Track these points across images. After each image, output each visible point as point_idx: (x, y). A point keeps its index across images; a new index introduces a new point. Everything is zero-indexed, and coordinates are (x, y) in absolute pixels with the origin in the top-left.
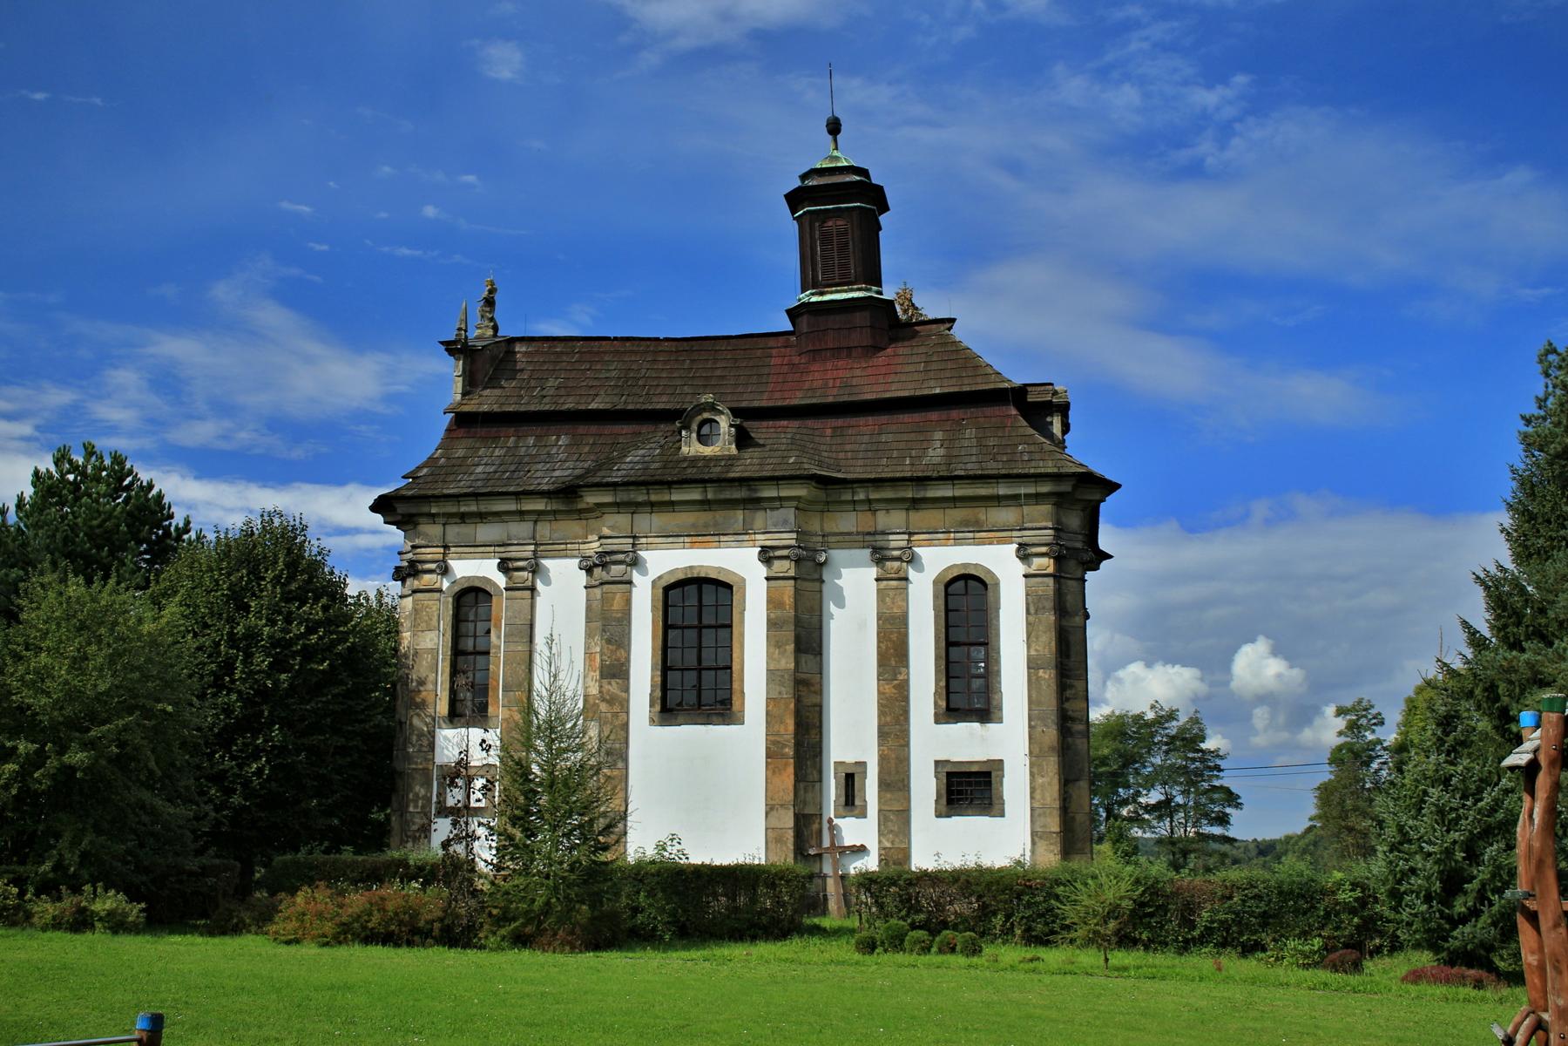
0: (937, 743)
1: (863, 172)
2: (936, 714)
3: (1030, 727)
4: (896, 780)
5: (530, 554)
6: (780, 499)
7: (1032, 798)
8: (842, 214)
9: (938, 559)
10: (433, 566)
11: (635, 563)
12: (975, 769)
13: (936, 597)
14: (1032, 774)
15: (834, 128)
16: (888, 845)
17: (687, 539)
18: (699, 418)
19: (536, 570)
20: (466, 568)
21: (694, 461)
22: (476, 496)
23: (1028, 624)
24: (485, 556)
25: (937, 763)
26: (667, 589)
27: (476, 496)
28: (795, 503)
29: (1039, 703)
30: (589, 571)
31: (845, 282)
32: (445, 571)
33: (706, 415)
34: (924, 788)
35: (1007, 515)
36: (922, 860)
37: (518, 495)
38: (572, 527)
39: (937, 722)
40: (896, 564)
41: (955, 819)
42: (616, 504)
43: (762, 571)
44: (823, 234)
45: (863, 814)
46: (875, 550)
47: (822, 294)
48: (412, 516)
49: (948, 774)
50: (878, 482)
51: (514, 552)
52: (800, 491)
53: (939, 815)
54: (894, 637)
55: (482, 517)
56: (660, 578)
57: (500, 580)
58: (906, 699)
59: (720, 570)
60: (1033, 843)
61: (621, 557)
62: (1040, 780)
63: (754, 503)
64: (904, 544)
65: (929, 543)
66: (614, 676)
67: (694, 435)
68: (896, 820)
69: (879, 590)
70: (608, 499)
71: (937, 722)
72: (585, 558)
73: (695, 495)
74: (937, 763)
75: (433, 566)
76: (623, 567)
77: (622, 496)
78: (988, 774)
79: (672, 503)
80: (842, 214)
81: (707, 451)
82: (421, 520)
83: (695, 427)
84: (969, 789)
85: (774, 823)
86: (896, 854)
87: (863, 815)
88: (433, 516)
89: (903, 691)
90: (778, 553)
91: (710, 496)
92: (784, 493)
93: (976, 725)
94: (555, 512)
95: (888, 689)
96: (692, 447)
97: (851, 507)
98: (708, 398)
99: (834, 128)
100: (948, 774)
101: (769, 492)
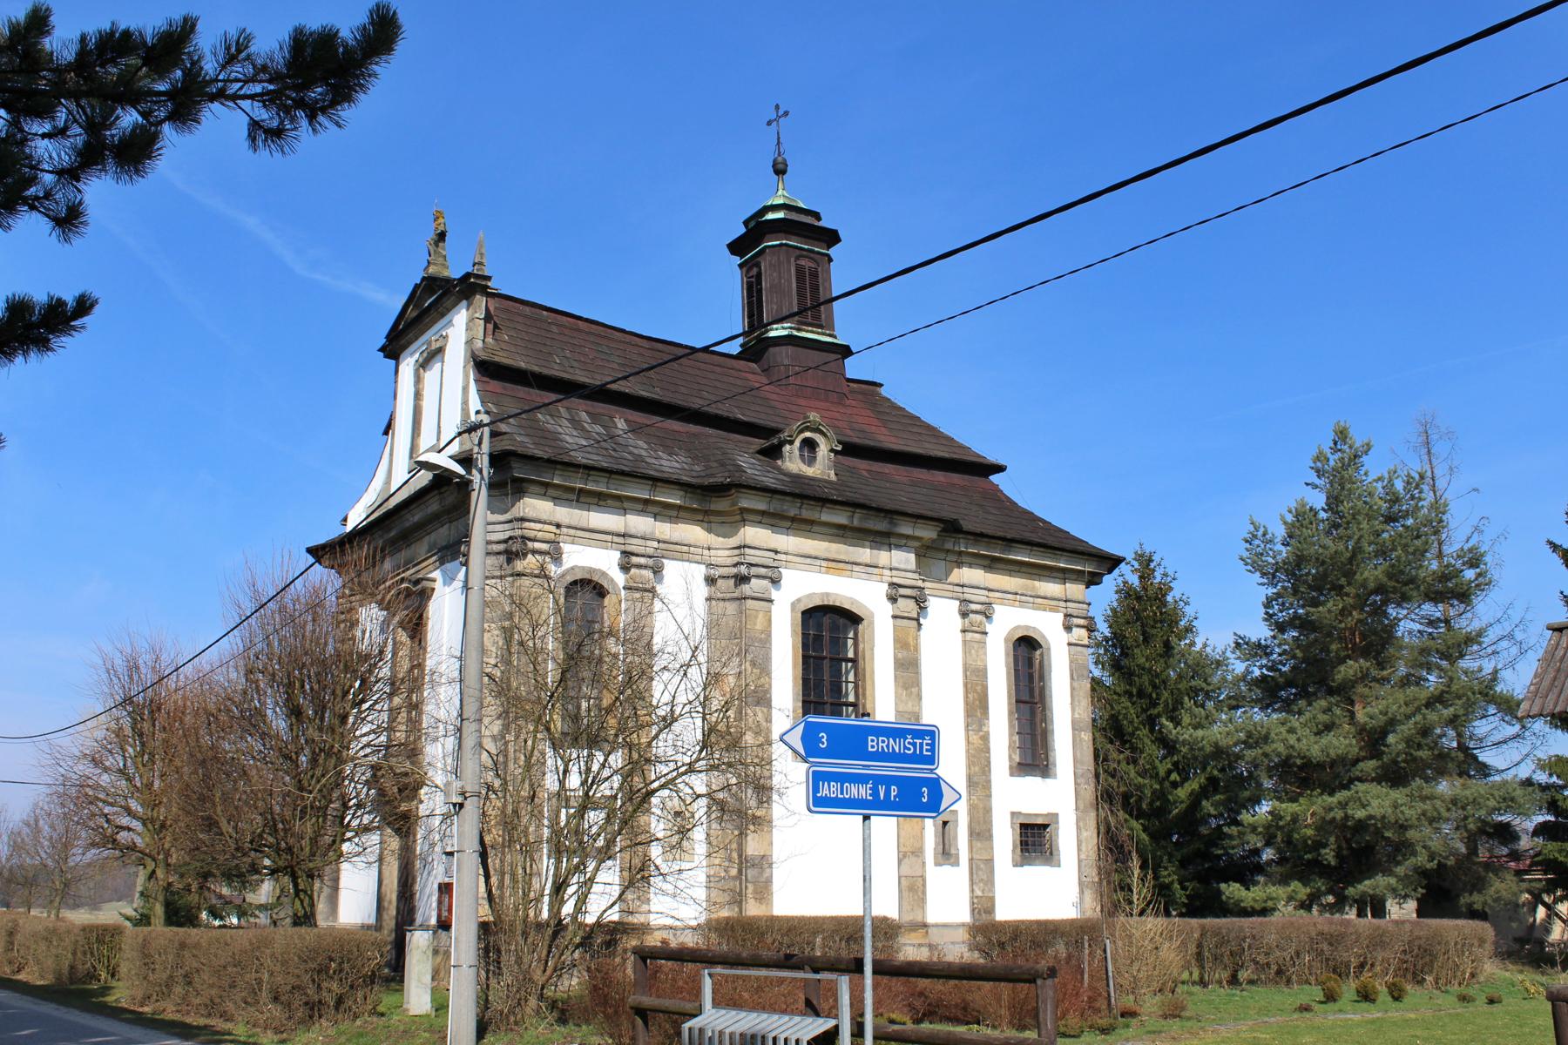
0: (1017, 796)
1: (817, 216)
2: (1011, 767)
3: (1076, 783)
4: (981, 832)
5: (650, 551)
6: (908, 537)
7: (1079, 850)
8: (784, 251)
9: (1008, 620)
10: (544, 547)
11: (775, 582)
12: (1040, 821)
13: (1007, 654)
14: (1078, 828)
15: (780, 170)
16: (979, 893)
17: (824, 564)
18: (808, 434)
19: (657, 571)
20: (580, 557)
21: (798, 478)
22: (609, 472)
23: (1073, 689)
24: (604, 545)
25: (1013, 814)
26: (804, 613)
27: (609, 472)
28: (917, 544)
29: (1082, 763)
30: (711, 581)
31: (818, 324)
32: (557, 557)
33: (808, 434)
34: (1004, 839)
35: (1051, 588)
36: (1005, 912)
37: (656, 481)
38: (692, 533)
39: (1012, 775)
40: (979, 618)
41: (1026, 868)
42: (763, 513)
43: (888, 606)
44: (798, 271)
45: (956, 863)
46: (964, 601)
47: (799, 330)
48: (523, 480)
49: (1022, 825)
50: (979, 537)
51: (634, 545)
52: (928, 533)
53: (1015, 865)
54: (979, 688)
55: (599, 500)
56: (799, 600)
57: (620, 578)
58: (988, 751)
59: (853, 601)
60: (1082, 892)
61: (763, 571)
62: (1085, 834)
63: (883, 539)
64: (983, 599)
65: (1002, 601)
66: (758, 703)
67: (797, 452)
68: (982, 872)
69: (965, 642)
70: (761, 506)
71: (1012, 775)
72: (709, 565)
73: (840, 518)
74: (1013, 814)
75: (544, 547)
76: (765, 582)
77: (775, 505)
78: (1045, 826)
79: (812, 522)
80: (784, 251)
81: (810, 471)
82: (533, 488)
83: (797, 443)
84: (1034, 839)
85: (906, 870)
86: (983, 905)
87: (956, 863)
88: (547, 485)
89: (985, 738)
90: (902, 591)
91: (856, 523)
92: (918, 533)
93: (1039, 779)
94: (679, 508)
95: (974, 738)
96: (793, 462)
97: (943, 555)
98: (814, 416)
99: (780, 170)
100: (1022, 825)
101: (906, 529)
